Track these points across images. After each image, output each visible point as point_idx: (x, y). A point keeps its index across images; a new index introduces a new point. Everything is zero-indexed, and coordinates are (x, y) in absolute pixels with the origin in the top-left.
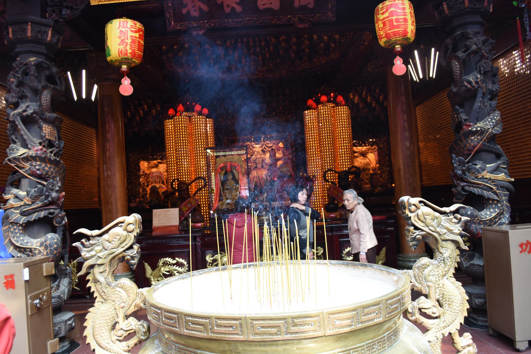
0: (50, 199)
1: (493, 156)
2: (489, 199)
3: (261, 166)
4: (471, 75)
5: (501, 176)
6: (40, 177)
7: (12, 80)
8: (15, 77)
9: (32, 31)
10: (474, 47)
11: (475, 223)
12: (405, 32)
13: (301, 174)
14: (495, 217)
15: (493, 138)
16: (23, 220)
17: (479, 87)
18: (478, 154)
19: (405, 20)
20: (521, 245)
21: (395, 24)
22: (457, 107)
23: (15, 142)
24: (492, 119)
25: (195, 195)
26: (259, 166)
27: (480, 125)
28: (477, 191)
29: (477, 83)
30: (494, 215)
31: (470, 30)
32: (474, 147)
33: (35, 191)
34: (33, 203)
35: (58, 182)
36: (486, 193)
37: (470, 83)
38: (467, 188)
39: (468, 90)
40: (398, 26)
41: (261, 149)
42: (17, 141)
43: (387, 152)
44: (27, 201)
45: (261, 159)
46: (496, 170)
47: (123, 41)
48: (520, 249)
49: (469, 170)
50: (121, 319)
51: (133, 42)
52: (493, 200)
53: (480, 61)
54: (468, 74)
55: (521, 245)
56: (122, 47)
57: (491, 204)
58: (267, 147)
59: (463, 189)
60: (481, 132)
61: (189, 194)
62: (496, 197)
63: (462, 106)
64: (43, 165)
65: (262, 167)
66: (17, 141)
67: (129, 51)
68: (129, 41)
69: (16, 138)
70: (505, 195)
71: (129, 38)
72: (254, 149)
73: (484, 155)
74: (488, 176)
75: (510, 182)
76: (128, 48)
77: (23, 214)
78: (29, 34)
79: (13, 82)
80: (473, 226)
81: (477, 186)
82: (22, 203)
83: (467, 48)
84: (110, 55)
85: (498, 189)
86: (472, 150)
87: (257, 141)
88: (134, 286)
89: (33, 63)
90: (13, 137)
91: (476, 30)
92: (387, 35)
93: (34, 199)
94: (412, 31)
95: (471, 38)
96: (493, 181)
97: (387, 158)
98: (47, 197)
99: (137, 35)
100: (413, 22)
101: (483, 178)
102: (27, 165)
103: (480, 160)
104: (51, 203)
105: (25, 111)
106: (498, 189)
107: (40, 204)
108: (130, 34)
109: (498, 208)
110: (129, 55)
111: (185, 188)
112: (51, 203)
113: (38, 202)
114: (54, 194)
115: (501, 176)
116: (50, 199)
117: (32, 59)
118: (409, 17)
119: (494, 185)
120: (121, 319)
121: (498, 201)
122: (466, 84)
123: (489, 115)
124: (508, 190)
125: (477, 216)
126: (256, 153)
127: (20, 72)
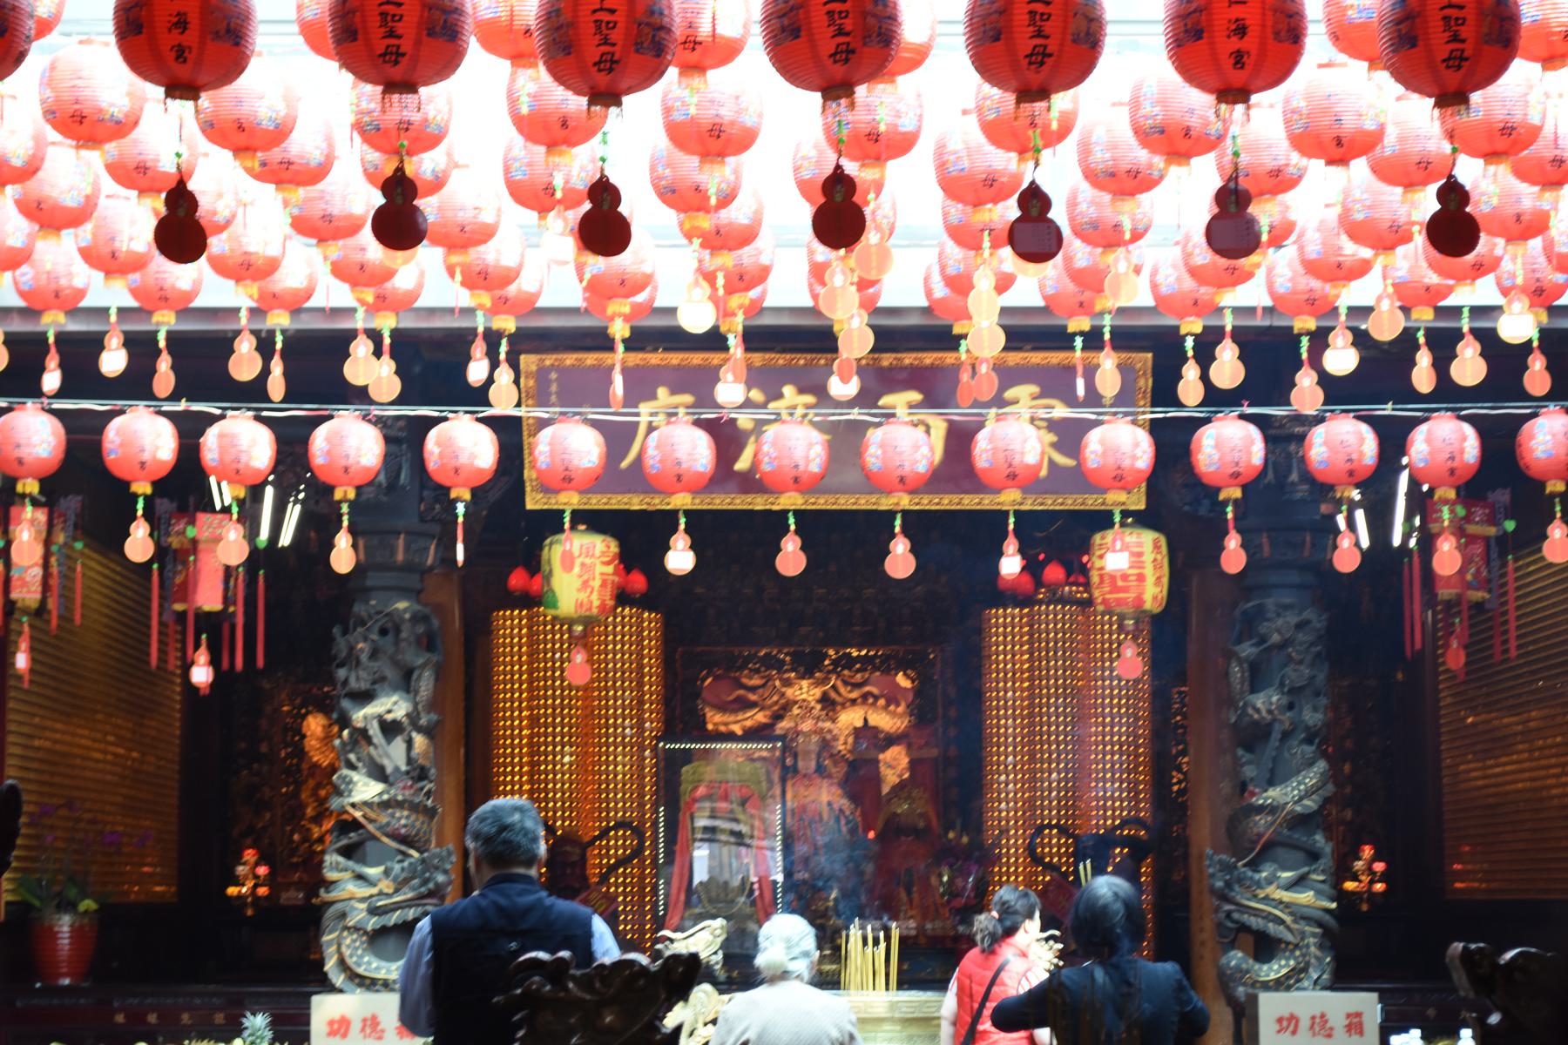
0: (431, 885)
1: (1300, 855)
2: (1280, 941)
3: (813, 764)
4: (1262, 694)
5: (1305, 897)
6: (405, 840)
7: (360, 645)
8: (365, 639)
9: (407, 549)
10: (1276, 638)
11: (1244, 984)
12: (1139, 600)
13: (951, 835)
14: (1287, 976)
15: (1301, 821)
16: (373, 923)
17: (1274, 720)
18: (1265, 852)
19: (1141, 578)
20: (1280, 1020)
21: (1120, 583)
22: (1240, 752)
23: (352, 767)
24: (1299, 783)
25: (604, 879)
26: (808, 765)
27: (1274, 794)
28: (1254, 922)
29: (1270, 712)
30: (1284, 971)
31: (1270, 603)
32: (1260, 836)
33: (403, 869)
34: (397, 891)
35: (450, 853)
36: (1272, 928)
37: (1258, 711)
38: (1236, 916)
39: (1256, 723)
40: (1125, 590)
41: (817, 692)
42: (360, 765)
43: (1348, 744)
44: (386, 886)
45: (815, 739)
46: (1298, 883)
47: (585, 584)
48: (1277, 1027)
49: (1240, 881)
50: (700, 1025)
51: (604, 584)
52: (1288, 943)
53: (1285, 665)
54: (1254, 690)
55: (1280, 1020)
56: (583, 596)
57: (1285, 950)
58: (846, 683)
59: (1228, 915)
60: (1272, 809)
61: (585, 878)
62: (1289, 937)
63: (1249, 749)
64: (413, 817)
65: (821, 770)
66: (360, 765)
67: (596, 603)
68: (597, 583)
69: (359, 759)
70: (1314, 935)
71: (598, 577)
72: (789, 692)
73: (1281, 852)
74: (1287, 896)
75: (1327, 911)
76: (595, 597)
77: (373, 911)
78: (400, 557)
79: (362, 650)
80: (1241, 989)
81: (1256, 913)
82: (375, 891)
83: (1263, 640)
84: (554, 606)
85: (1295, 921)
86: (1257, 842)
87: (808, 666)
88: (716, 993)
89: (407, 616)
90: (352, 757)
91: (1287, 600)
92: (1104, 602)
93: (400, 886)
94: (1155, 598)
95: (1268, 620)
96: (1286, 906)
97: (1347, 768)
98: (425, 882)
99: (610, 569)
100: (1159, 578)
101: (1267, 899)
102: (384, 819)
103: (1274, 861)
104: (431, 894)
105: (389, 712)
106: (1295, 921)
107: (410, 895)
108: (600, 569)
109: (1295, 959)
110: (595, 611)
111: (575, 858)
112: (431, 894)
113: (405, 889)
114: (441, 878)
115: (1305, 897)
116: (431, 885)
117: (402, 605)
118: (1149, 572)
119: (1291, 914)
120: (700, 1025)
121: (1296, 946)
122: (1250, 711)
123: (1299, 772)
124: (1320, 924)
125: (1248, 971)
126: (796, 711)
127: (376, 628)
